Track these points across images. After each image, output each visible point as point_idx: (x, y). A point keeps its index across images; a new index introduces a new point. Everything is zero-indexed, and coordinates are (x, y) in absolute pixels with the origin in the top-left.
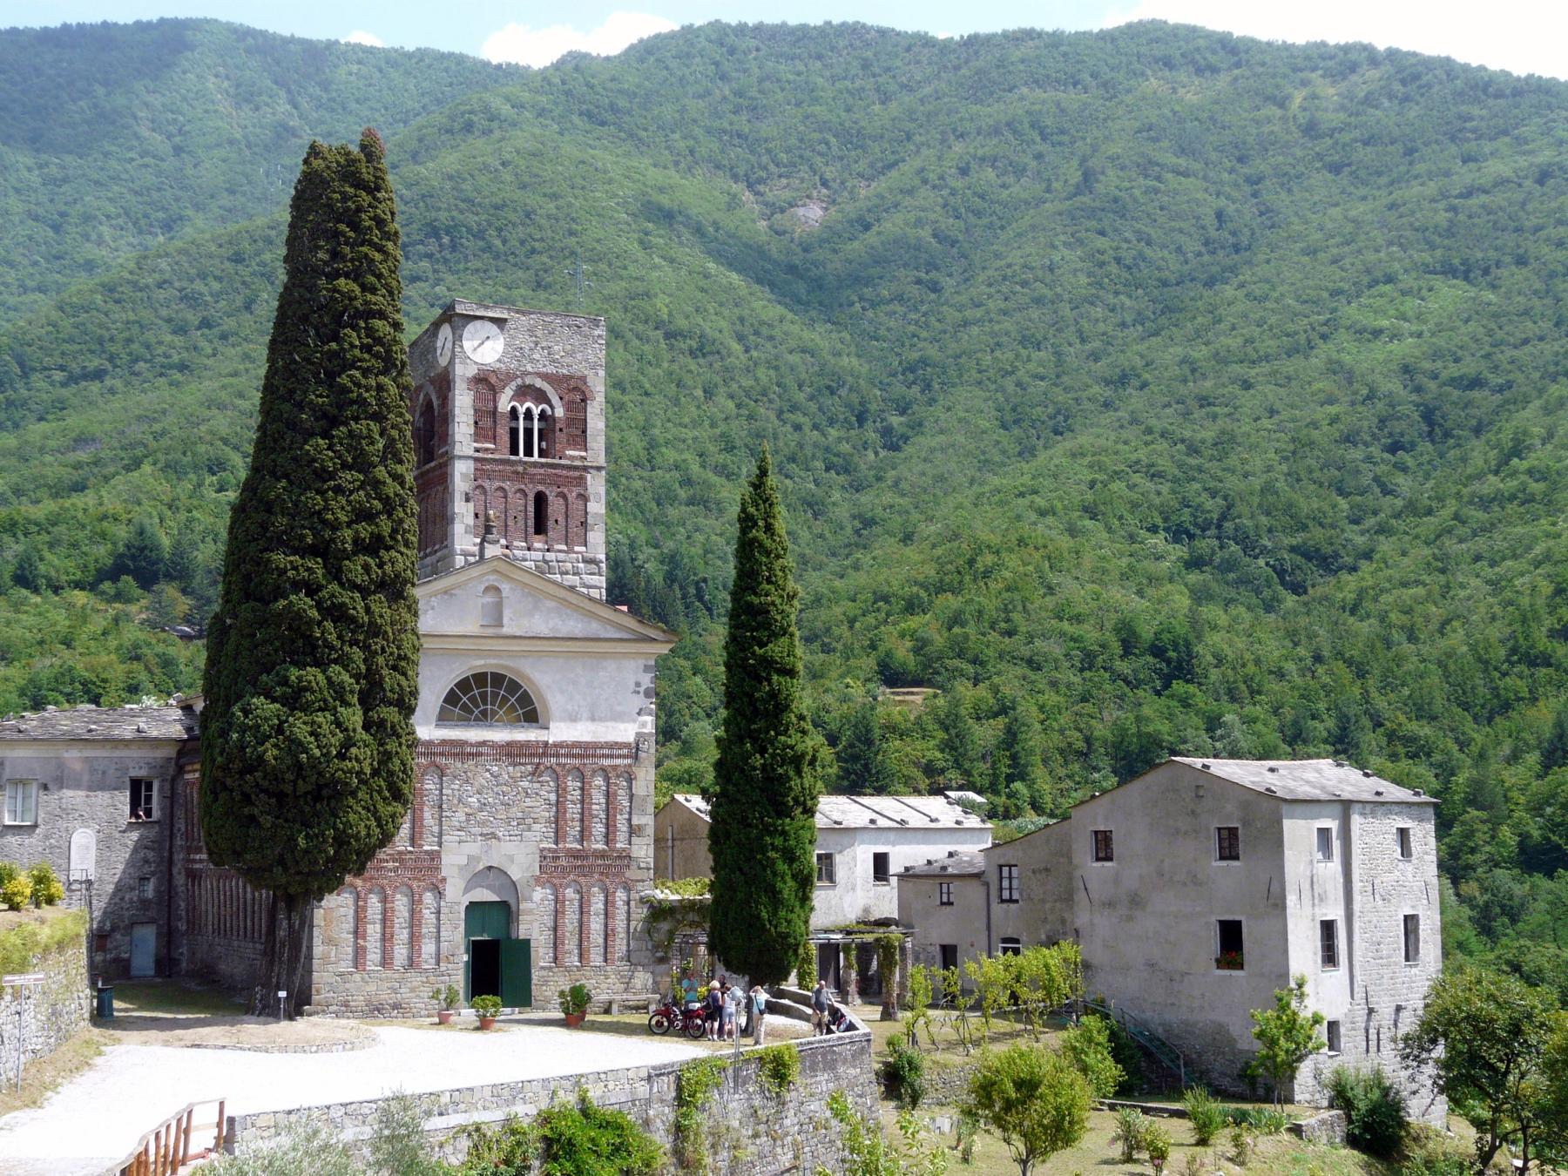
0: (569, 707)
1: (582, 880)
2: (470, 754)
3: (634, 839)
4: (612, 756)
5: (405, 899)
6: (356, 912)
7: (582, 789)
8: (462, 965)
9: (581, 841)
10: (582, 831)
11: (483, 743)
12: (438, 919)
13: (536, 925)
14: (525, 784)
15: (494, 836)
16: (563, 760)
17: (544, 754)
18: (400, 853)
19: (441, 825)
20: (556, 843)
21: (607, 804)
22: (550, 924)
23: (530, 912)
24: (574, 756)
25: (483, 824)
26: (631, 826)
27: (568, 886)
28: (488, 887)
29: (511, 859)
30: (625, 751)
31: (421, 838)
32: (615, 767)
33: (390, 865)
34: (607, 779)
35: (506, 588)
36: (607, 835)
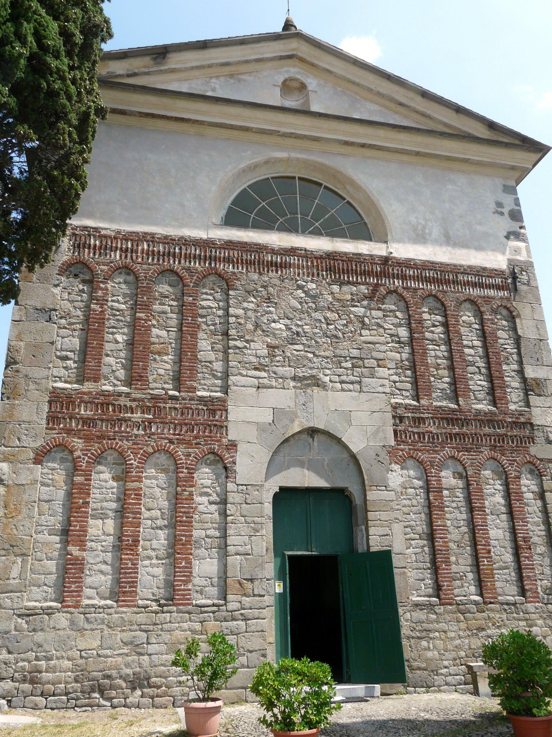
0: (413, 219)
1: (464, 456)
2: (272, 264)
3: (533, 399)
4: (481, 286)
5: (162, 476)
6: (70, 495)
7: (446, 325)
8: (269, 600)
9: (455, 397)
10: (454, 383)
11: (292, 251)
12: (224, 514)
13: (397, 528)
14: (360, 311)
15: (317, 383)
16: (413, 284)
17: (384, 274)
18: (155, 398)
19: (226, 360)
20: (417, 398)
21: (485, 347)
22: (422, 527)
23: (386, 505)
24: (428, 280)
25: (296, 362)
26: (524, 380)
27: (442, 466)
28: (313, 467)
29: (347, 416)
30: (499, 281)
31: (192, 377)
32: (488, 299)
33: (137, 416)
34: (479, 314)
35: (312, 83)
36: (492, 391)
